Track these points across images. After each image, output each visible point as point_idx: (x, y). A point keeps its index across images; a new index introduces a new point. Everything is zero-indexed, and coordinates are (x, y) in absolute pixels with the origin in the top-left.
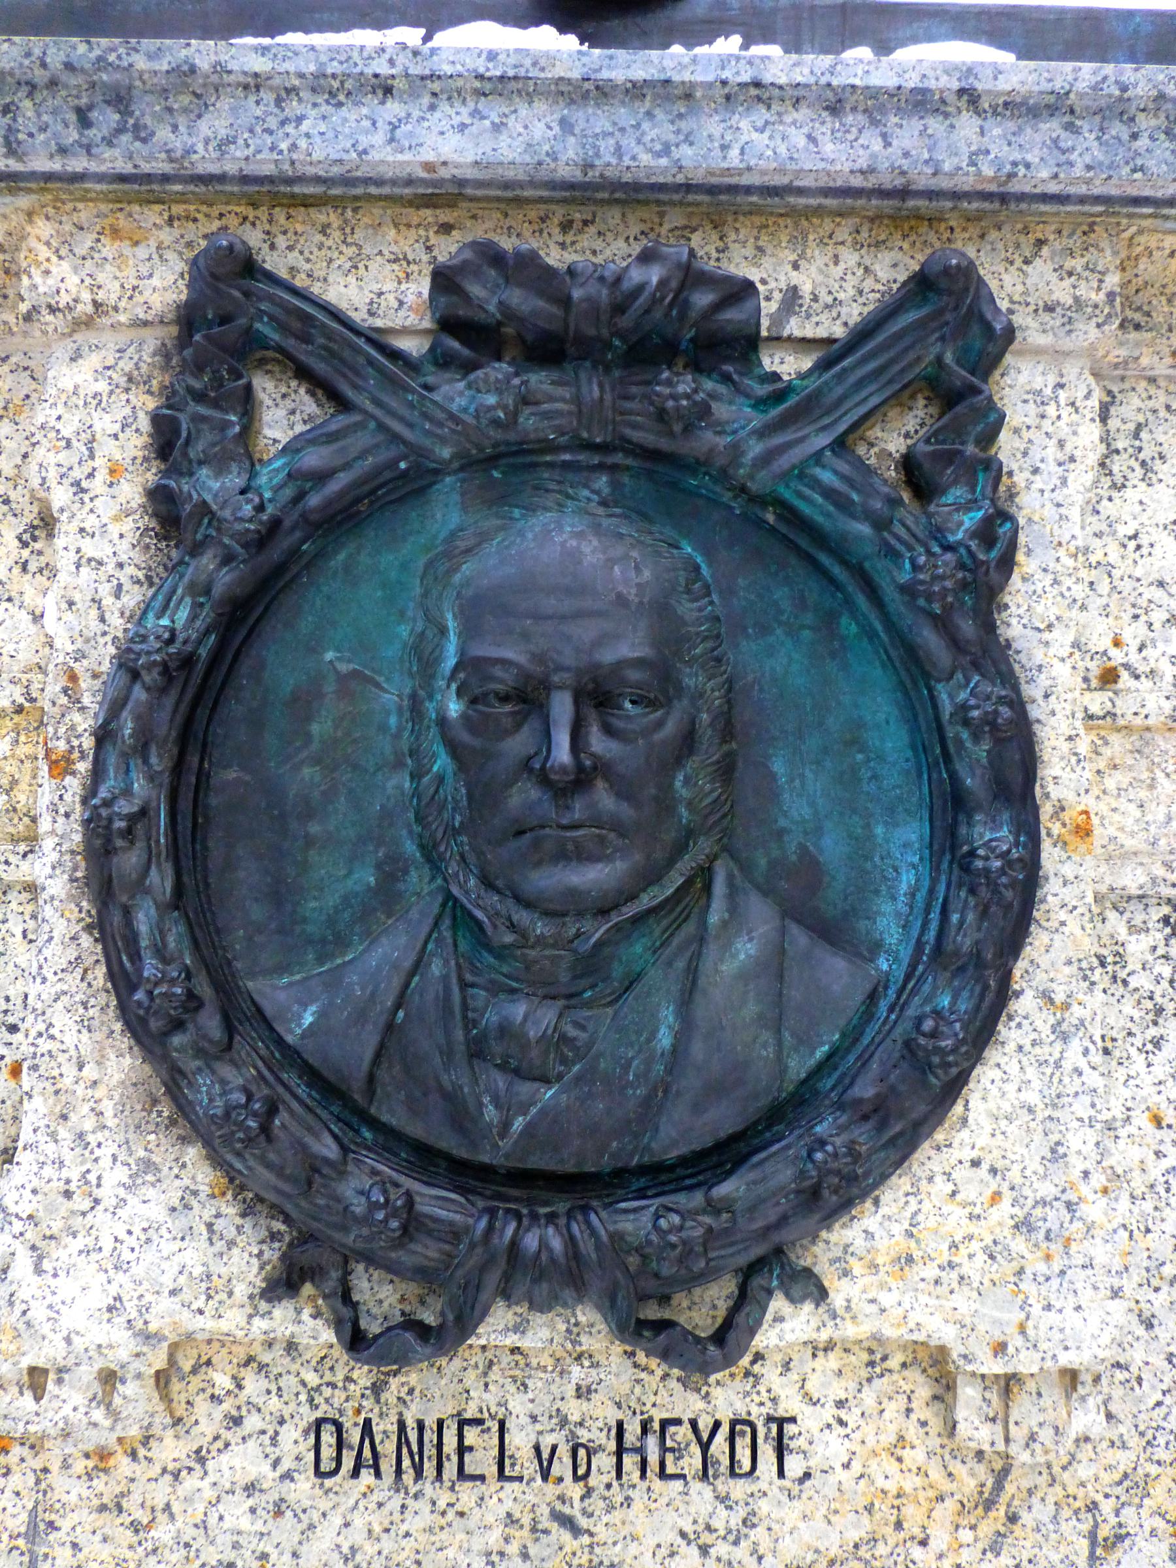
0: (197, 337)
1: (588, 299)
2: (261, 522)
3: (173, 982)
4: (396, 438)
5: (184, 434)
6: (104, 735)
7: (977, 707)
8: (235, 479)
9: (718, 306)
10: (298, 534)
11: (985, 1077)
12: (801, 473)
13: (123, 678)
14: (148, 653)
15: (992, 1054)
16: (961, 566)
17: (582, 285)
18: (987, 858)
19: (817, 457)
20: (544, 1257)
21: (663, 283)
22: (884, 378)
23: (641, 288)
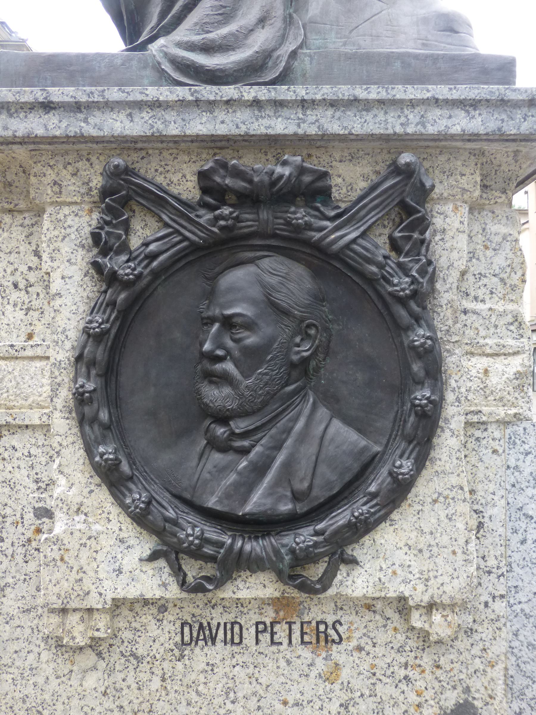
0: (107, 200)
1: (261, 181)
2: (135, 275)
3: (110, 453)
4: (186, 239)
5: (104, 240)
6: (79, 359)
7: (417, 341)
8: (124, 258)
9: (313, 182)
10: (149, 278)
11: (421, 482)
12: (347, 246)
13: (85, 337)
14: (94, 329)
15: (424, 472)
16: (412, 283)
17: (258, 176)
18: (420, 400)
19: (354, 241)
20: (253, 554)
21: (290, 175)
22: (381, 207)
23: (281, 177)
